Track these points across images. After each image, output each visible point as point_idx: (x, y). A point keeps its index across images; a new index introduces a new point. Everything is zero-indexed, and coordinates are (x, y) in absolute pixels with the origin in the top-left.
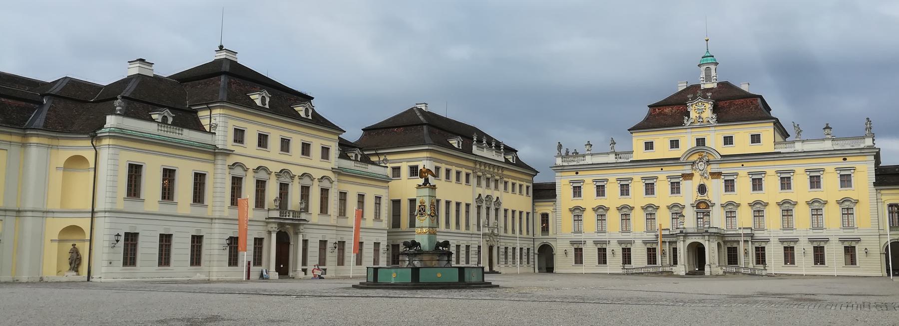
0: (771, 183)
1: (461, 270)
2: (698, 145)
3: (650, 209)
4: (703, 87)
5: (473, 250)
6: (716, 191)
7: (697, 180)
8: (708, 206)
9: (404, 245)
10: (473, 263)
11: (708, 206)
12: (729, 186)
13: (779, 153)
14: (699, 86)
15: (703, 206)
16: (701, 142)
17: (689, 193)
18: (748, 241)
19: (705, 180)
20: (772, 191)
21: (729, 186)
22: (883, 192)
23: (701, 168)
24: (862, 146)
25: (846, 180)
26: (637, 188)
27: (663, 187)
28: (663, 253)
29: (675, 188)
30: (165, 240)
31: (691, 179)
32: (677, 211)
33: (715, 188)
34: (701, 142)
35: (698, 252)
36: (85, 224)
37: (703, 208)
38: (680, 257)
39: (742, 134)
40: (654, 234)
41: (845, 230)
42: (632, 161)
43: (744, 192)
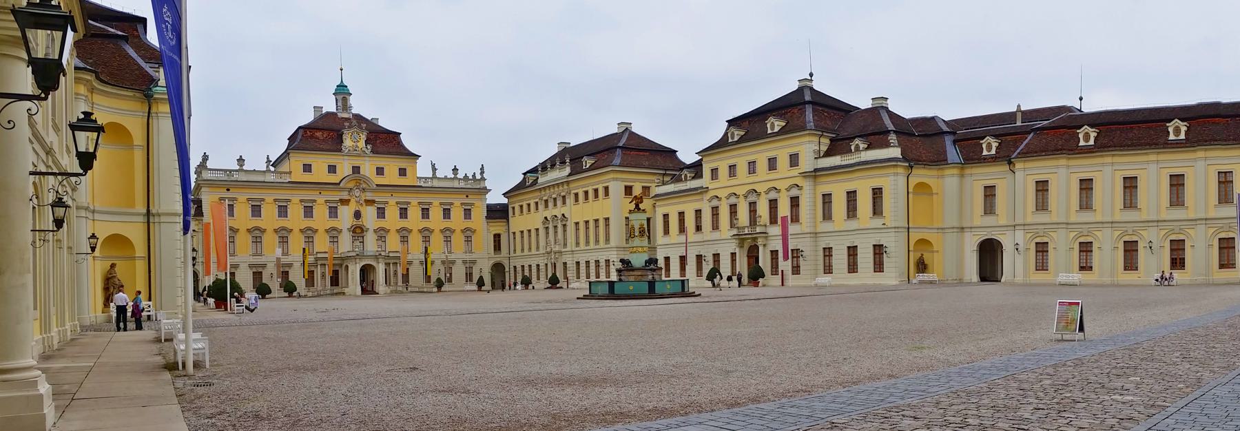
0: (414, 213)
1: (611, 284)
2: (353, 173)
3: (309, 232)
4: (340, 115)
5: (542, 267)
6: (370, 217)
7: (353, 207)
8: (363, 231)
9: (620, 261)
10: (603, 278)
11: (363, 231)
12: (381, 213)
13: (421, 187)
14: (333, 113)
15: (358, 231)
16: (356, 170)
17: (346, 216)
18: (397, 263)
19: (360, 207)
20: (415, 220)
21: (381, 213)
22: (491, 224)
23: (357, 195)
24: (478, 187)
25: (468, 214)
26: (296, 211)
27: (321, 211)
28: (323, 276)
29: (333, 212)
30: (852, 251)
31: (348, 205)
32: (334, 234)
33: (369, 213)
34: (356, 170)
35: (366, 272)
36: (134, 233)
37: (358, 232)
38: (342, 279)
39: (392, 165)
40: (312, 256)
41: (468, 254)
42: (289, 182)
43: (392, 219)
